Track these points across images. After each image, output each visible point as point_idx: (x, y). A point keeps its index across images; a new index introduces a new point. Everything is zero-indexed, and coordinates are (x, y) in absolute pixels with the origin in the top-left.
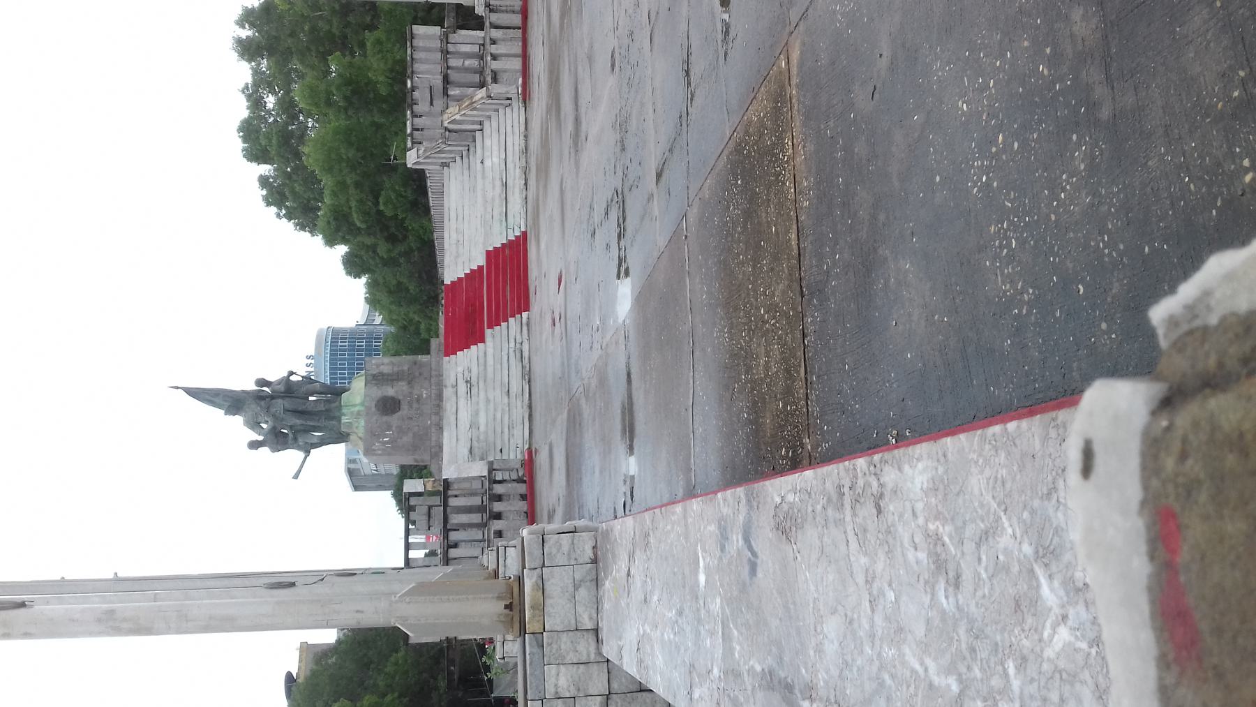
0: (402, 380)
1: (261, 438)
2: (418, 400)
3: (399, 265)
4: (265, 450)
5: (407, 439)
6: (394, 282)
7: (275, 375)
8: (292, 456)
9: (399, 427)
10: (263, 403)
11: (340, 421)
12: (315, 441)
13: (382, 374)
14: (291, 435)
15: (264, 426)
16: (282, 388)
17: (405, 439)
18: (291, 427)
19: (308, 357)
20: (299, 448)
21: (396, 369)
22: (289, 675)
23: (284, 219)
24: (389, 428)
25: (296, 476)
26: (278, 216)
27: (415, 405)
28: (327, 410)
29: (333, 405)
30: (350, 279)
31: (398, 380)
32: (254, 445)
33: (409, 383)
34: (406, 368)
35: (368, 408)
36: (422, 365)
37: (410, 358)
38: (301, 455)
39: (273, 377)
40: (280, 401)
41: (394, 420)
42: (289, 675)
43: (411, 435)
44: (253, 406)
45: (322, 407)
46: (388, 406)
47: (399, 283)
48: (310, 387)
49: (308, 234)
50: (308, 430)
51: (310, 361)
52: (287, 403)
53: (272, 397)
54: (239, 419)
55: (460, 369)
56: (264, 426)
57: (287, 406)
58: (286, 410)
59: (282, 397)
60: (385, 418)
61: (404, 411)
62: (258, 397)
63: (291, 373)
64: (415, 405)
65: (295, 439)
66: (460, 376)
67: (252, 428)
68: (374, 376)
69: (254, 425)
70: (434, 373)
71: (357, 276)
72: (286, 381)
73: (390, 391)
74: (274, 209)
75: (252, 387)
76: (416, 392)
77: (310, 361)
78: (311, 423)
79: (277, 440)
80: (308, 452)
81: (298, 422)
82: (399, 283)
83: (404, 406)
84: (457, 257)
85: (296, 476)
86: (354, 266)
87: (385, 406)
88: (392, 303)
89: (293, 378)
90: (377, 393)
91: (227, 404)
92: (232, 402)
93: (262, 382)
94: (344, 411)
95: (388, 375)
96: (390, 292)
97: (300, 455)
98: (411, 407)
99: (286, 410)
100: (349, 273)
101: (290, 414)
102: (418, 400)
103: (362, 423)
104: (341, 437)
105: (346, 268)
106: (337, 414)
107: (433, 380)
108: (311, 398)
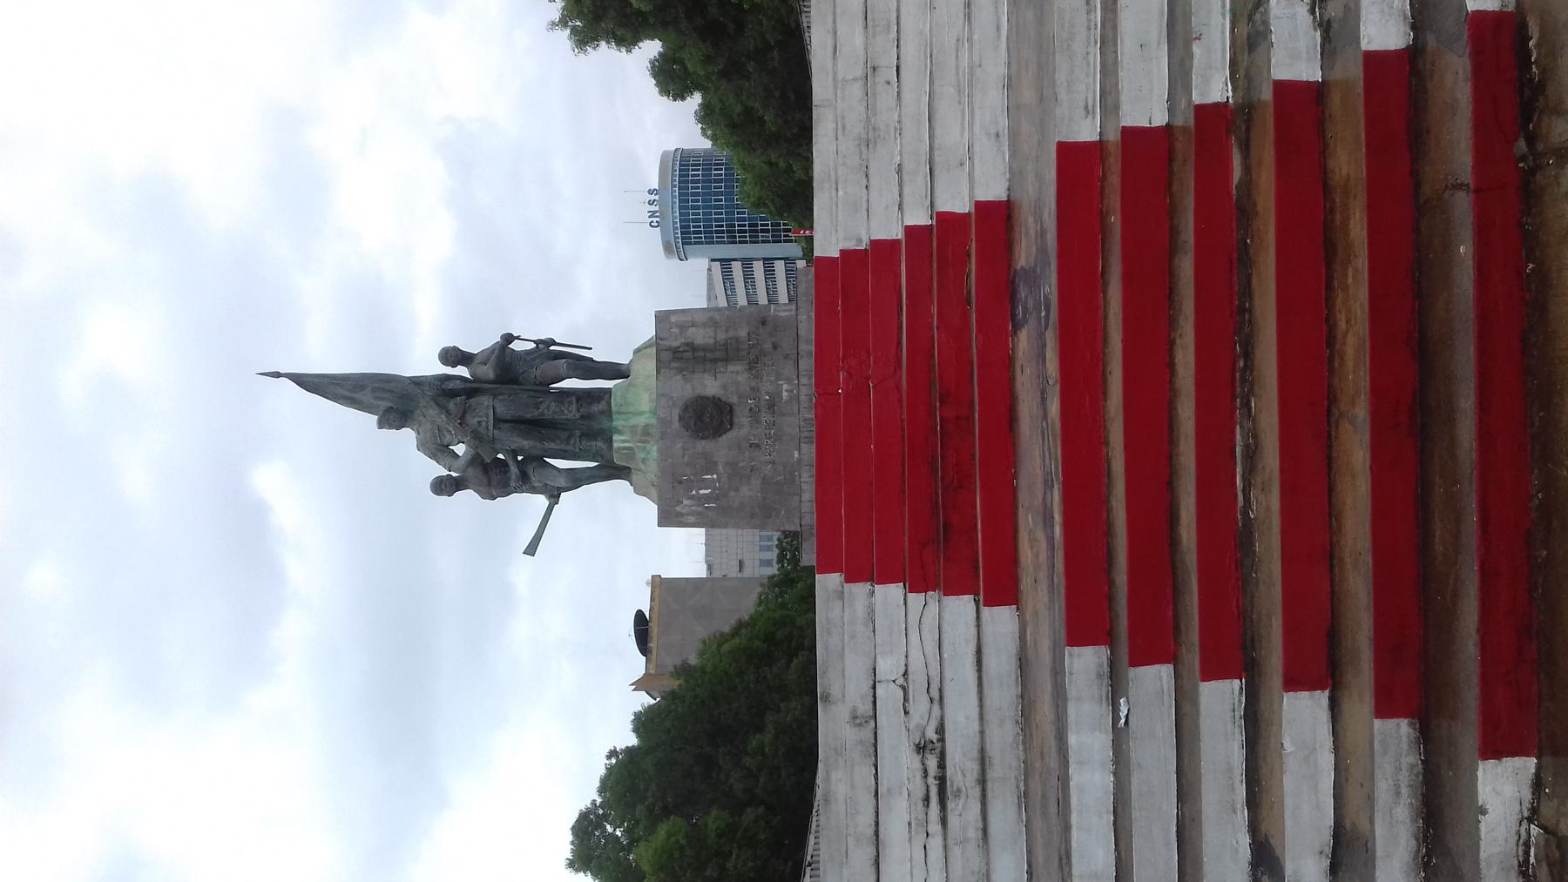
0: (739, 359)
2: (771, 406)
4: (468, 497)
5: (749, 492)
6: (738, 109)
7: (478, 342)
10: (451, 406)
13: (692, 347)
14: (514, 469)
15: (460, 449)
16: (488, 372)
17: (745, 491)
19: (651, 192)
20: (534, 490)
21: (722, 336)
22: (640, 614)
24: (710, 466)
25: (531, 550)
27: (765, 417)
29: (596, 408)
31: (727, 360)
32: (444, 487)
34: (743, 333)
35: (664, 423)
38: (542, 501)
39: (473, 347)
40: (485, 401)
41: (721, 448)
42: (640, 616)
43: (756, 482)
44: (433, 412)
45: (571, 412)
46: (707, 418)
47: (748, 111)
51: (653, 197)
53: (470, 390)
54: (408, 436)
55: (889, 667)
56: (460, 449)
57: (501, 410)
60: (701, 445)
61: (743, 428)
62: (442, 389)
63: (509, 338)
64: (765, 417)
66: (889, 695)
67: (433, 456)
68: (676, 353)
69: (437, 449)
71: (680, 94)
73: (711, 386)
76: (766, 386)
77: (653, 197)
79: (493, 475)
80: (554, 497)
81: (526, 444)
82: (748, 111)
83: (742, 418)
84: (868, 142)
85: (531, 550)
87: (699, 418)
89: (516, 346)
90: (684, 388)
91: (385, 404)
92: (389, 399)
93: (452, 356)
94: (618, 422)
95: (705, 349)
96: (733, 126)
98: (754, 413)
101: (507, 419)
102: (771, 406)
106: (605, 424)
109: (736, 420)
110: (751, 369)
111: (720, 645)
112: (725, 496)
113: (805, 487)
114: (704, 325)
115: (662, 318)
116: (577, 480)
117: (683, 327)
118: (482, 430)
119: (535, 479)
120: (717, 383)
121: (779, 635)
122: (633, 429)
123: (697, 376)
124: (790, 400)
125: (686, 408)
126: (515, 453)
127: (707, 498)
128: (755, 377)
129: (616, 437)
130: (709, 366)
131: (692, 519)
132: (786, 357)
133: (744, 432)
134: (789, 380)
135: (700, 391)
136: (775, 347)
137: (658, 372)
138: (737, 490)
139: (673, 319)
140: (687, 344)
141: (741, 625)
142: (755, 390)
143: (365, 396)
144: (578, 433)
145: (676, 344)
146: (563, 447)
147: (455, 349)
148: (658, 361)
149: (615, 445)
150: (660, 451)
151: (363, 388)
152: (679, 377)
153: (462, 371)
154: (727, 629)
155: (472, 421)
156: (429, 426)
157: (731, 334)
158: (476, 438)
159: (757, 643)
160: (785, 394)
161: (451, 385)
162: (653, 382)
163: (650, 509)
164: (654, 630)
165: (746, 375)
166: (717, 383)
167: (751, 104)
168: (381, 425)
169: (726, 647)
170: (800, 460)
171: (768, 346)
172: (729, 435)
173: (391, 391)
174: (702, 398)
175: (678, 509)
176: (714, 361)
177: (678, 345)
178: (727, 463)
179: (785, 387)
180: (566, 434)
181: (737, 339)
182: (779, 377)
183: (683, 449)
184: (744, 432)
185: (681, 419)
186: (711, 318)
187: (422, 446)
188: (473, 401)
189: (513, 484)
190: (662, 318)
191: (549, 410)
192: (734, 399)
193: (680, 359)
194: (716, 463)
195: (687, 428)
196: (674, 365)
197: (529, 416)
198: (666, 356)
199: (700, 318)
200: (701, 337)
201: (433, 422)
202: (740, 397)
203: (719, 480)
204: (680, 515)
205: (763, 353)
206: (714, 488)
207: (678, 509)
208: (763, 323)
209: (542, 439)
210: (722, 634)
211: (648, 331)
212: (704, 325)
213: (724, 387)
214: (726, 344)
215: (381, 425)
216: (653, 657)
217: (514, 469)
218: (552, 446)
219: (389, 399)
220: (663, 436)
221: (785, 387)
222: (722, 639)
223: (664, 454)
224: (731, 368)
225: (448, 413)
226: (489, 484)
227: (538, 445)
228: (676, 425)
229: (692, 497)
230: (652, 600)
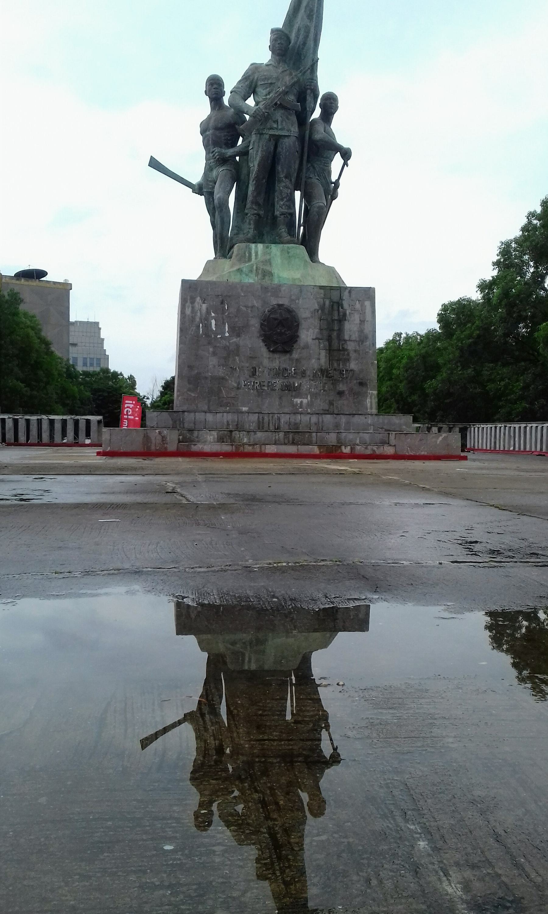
1: (226, 100)
2: (289, 388)
3: (464, 367)
4: (204, 109)
5: (212, 365)
6: (440, 361)
7: (341, 129)
8: (193, 161)
9: (237, 351)
10: (291, 98)
11: (254, 241)
12: (217, 195)
13: (342, 319)
14: (230, 152)
15: (251, 102)
16: (319, 135)
17: (213, 361)
18: (244, 153)
20: (209, 169)
21: (351, 346)
23: (525, 221)
24: (236, 331)
25: (154, 164)
26: (532, 215)
27: (278, 382)
28: (275, 218)
29: (283, 230)
30: (437, 309)
31: (330, 350)
32: (214, 87)
33: (323, 372)
34: (353, 365)
35: (276, 290)
36: (358, 395)
37: (373, 374)
38: (196, 177)
40: (295, 130)
41: (252, 341)
42: (43, 274)
43: (221, 372)
44: (287, 79)
46: (280, 330)
47: (437, 368)
48: (319, 190)
49: (495, 258)
50: (238, 177)
52: (289, 144)
53: (302, 117)
54: (264, 56)
58: (277, 139)
59: (301, 138)
60: (255, 324)
61: (269, 361)
63: (346, 155)
64: (278, 382)
65: (223, 161)
67: (246, 77)
68: (339, 304)
69: (251, 83)
70: (343, 419)
71: (442, 318)
72: (331, 147)
73: (308, 334)
74: (539, 210)
75: (324, 87)
76: (306, 384)
78: (251, 188)
79: (223, 133)
80: (198, 189)
81: (254, 164)
82: (437, 368)
83: (280, 361)
85: (154, 164)
86: (456, 316)
87: (282, 323)
88: (410, 358)
89: (337, 161)
90: (307, 310)
93: (330, 105)
94: (275, 249)
95: (340, 331)
96: (424, 357)
97: (196, 175)
98: (281, 373)
99: (277, 139)
100: (445, 308)
101: (272, 154)
103: (250, 280)
104: (223, 245)
105: (451, 304)
107: (328, 418)
108: (298, 194)
109: (276, 356)
110: (322, 371)
111: (33, 328)
112: (209, 343)
113: (219, 415)
114: (361, 331)
115: (368, 295)
116: (216, 209)
117: (363, 312)
118: (270, 123)
119: (220, 172)
120: (309, 340)
121: (40, 373)
122: (269, 262)
123: (316, 322)
124: (294, 406)
125: (289, 311)
126: (244, 153)
127: (207, 326)
128: (315, 375)
129: (260, 246)
130: (325, 333)
131: (188, 311)
132: (331, 403)
133: (266, 362)
134: (310, 405)
135: (304, 325)
136: (341, 394)
137: (321, 287)
138: (214, 354)
139: (367, 303)
140: (345, 315)
141: (47, 344)
142: (303, 374)
143: (301, 19)
144: (262, 213)
145: (345, 304)
146: (250, 198)
147: (336, 108)
148: (332, 288)
149: (253, 246)
150: (251, 285)
151: (310, 17)
152: (317, 307)
153: (317, 113)
154: (43, 334)
155: (279, 115)
156: (275, 75)
157: (353, 355)
158: (262, 118)
159: (34, 355)
160: (298, 401)
161: (309, 99)
162: (309, 282)
163: (194, 273)
164: (34, 283)
165: (316, 366)
166: (309, 340)
167: (444, 370)
168: (273, 31)
169: (32, 333)
170: (242, 412)
171: (341, 387)
172: (264, 350)
173: (304, 44)
174: (298, 326)
175: (198, 299)
176: (329, 339)
177: (344, 307)
178: (238, 346)
179: (305, 401)
180: (261, 201)
181: (348, 360)
182: (315, 396)
183: (253, 307)
184: (266, 362)
185: (280, 306)
186: (366, 338)
187: (255, 68)
188: (294, 118)
189: (217, 150)
190: (368, 295)
191: (282, 186)
192: (295, 355)
193: (332, 306)
194: (238, 336)
195: (273, 311)
196: (327, 302)
197: (279, 168)
198: (335, 298)
199: (367, 328)
200: (351, 328)
201: (278, 79)
202: (297, 360)
203: (223, 338)
204: (193, 302)
205: (335, 382)
206: (216, 334)
207: (199, 298)
208: (361, 384)
209: (257, 178)
210: (40, 330)
211: (351, 280)
212: (361, 331)
213: (306, 347)
214: (344, 350)
215: (274, 32)
216: (14, 281)
217: (230, 152)
218: (251, 188)
219: (295, 46)
220: (265, 289)
221: (305, 401)
222: (38, 331)
223: (248, 289)
224: (323, 353)
225: (286, 93)
226: (216, 129)
227: (253, 176)
228: (274, 301)
229: (208, 312)
230: (55, 283)
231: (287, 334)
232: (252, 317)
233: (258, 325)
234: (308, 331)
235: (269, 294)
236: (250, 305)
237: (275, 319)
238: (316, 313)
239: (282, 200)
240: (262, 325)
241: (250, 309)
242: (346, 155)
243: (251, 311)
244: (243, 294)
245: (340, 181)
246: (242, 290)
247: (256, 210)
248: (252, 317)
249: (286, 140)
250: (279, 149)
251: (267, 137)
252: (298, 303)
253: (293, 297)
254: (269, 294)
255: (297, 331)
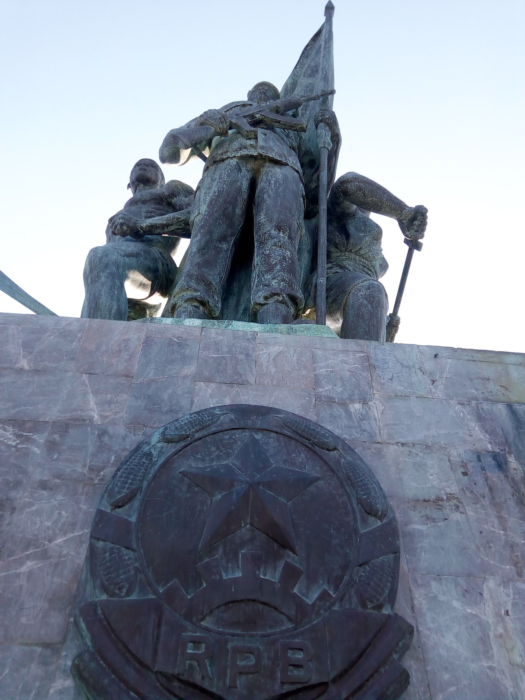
63: (414, 223)
197: (261, 218)
231: (302, 611)
232: (44, 485)
233: (71, 548)
234: (472, 593)
235: (190, 369)
236: (54, 413)
237: (212, 481)
238: (495, 476)
239: (270, 269)
240: (103, 527)
241: (41, 438)
242: (414, 223)
243: (51, 447)
244: (24, 364)
245: (399, 314)
246: (27, 346)
247: (196, 290)
248: (44, 485)
249: (278, 171)
250: (261, 185)
251: (234, 162)
252: (364, 417)
253: (325, 389)
254: (190, 369)
255: (387, 582)
